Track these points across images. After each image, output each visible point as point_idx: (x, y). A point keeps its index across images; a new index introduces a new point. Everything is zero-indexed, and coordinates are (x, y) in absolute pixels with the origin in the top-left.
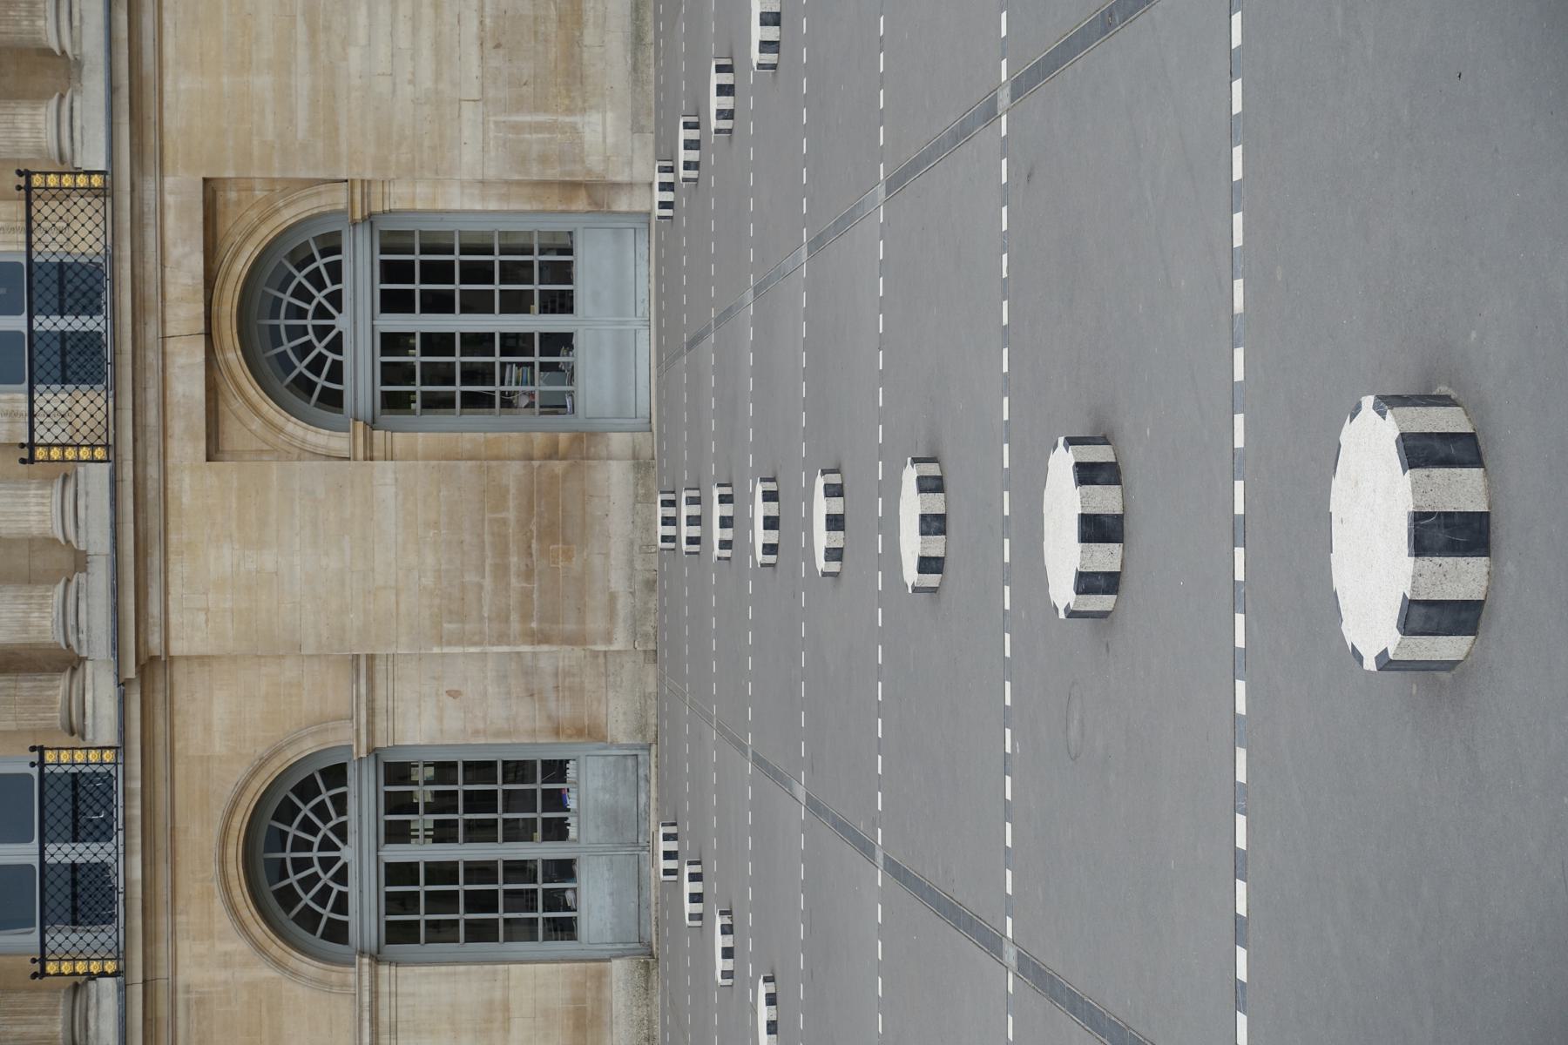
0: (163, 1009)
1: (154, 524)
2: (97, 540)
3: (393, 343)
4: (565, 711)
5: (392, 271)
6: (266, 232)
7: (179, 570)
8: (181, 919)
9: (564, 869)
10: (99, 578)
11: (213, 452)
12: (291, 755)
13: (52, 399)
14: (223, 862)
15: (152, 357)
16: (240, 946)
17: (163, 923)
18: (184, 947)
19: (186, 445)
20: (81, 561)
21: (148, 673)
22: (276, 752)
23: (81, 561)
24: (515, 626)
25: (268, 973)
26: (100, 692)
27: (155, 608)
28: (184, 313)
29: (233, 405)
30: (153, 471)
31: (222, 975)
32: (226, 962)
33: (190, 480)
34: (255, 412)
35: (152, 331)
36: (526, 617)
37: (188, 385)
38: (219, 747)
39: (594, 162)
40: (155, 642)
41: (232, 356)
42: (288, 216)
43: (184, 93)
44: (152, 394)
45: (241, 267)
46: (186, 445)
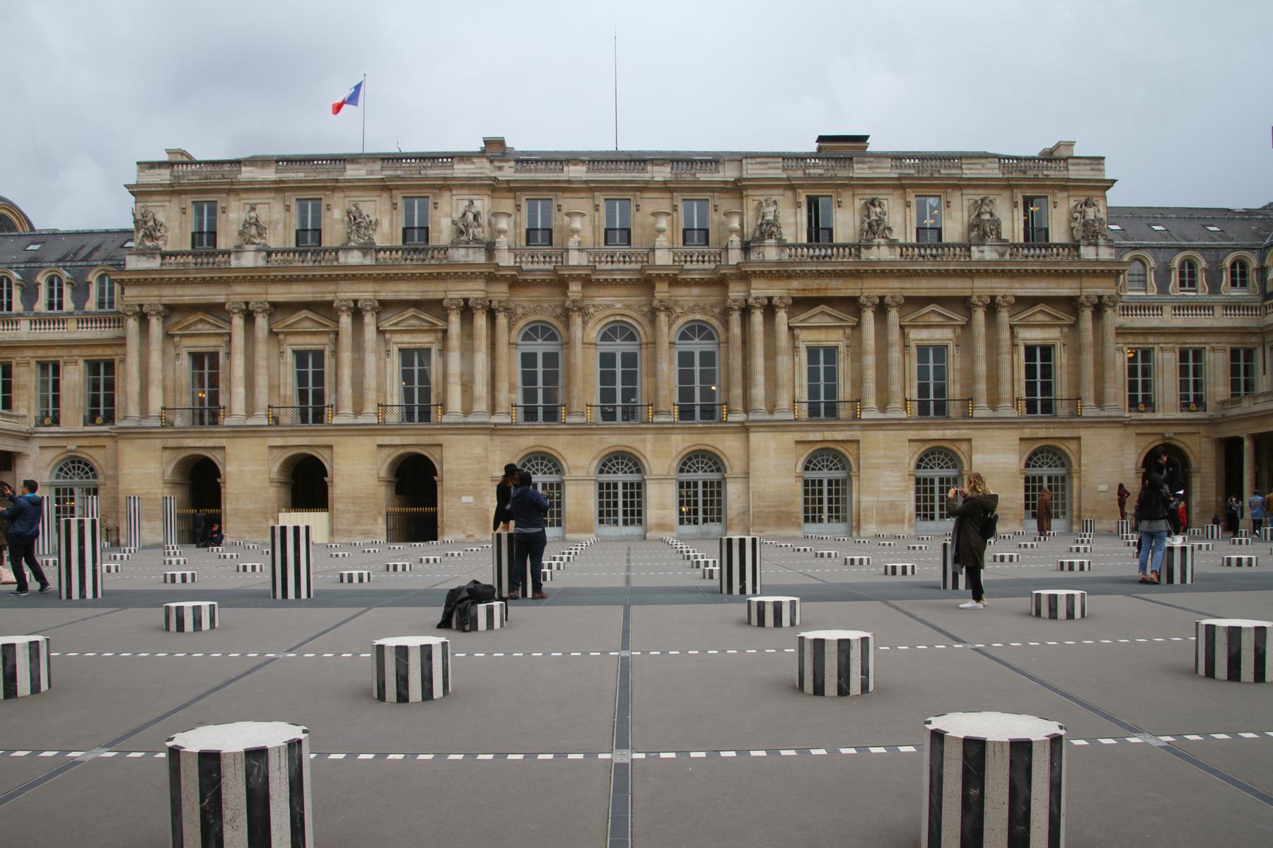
2: (777, 416)
3: (821, 483)
5: (837, 482)
6: (847, 454)
7: (770, 434)
10: (768, 417)
11: (797, 442)
12: (725, 460)
13: (805, 407)
18: (680, 437)
19: (798, 436)
20: (771, 412)
21: (745, 429)
23: (771, 412)
26: (740, 417)
28: (829, 435)
29: (807, 446)
33: (790, 438)
34: (806, 452)
41: (818, 446)
42: (851, 459)
43: (880, 435)
45: (839, 448)
46: (798, 436)
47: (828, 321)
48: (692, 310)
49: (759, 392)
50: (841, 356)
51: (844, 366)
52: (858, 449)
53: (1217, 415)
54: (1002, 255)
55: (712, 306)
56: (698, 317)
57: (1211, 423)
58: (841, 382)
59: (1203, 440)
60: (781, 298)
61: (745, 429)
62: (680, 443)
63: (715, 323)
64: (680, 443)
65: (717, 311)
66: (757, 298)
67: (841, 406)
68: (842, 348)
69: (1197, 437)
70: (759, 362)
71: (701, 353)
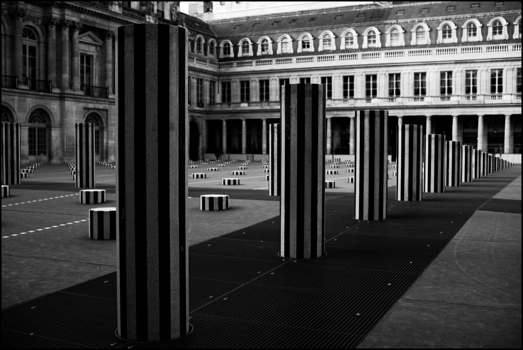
0: (24, 95)
1: (78, 100)
4: (55, 154)
7: (73, 103)
8: (34, 99)
9: (35, 154)
14: (40, 105)
15: (93, 101)
16: (31, 106)
17: (33, 96)
18: (30, 99)
21: (62, 98)
22: (51, 114)
24: (68, 147)
25: (28, 110)
27: (70, 99)
30: (82, 100)
31: (28, 104)
32: (29, 105)
33: (82, 105)
35: (95, 102)
36: (69, 148)
37: (91, 106)
38: (52, 106)
39: (109, 157)
40: (66, 99)
41: (91, 111)
42: (103, 119)
44: (89, 101)
45: (99, 113)
47: (89, 40)
48: (28, 20)
49: (66, 76)
50: (94, 61)
51: (96, 67)
52: (107, 114)
53: (208, 109)
54: (156, 22)
55: (38, 18)
56: (31, 24)
57: (207, 113)
58: (94, 76)
59: (203, 120)
60: (78, 23)
61: (62, 98)
62: (31, 103)
63: (38, 29)
64: (31, 103)
65: (40, 22)
66: (68, 21)
67: (94, 89)
68: (95, 57)
69: (201, 119)
70: (67, 59)
71: (30, 47)
